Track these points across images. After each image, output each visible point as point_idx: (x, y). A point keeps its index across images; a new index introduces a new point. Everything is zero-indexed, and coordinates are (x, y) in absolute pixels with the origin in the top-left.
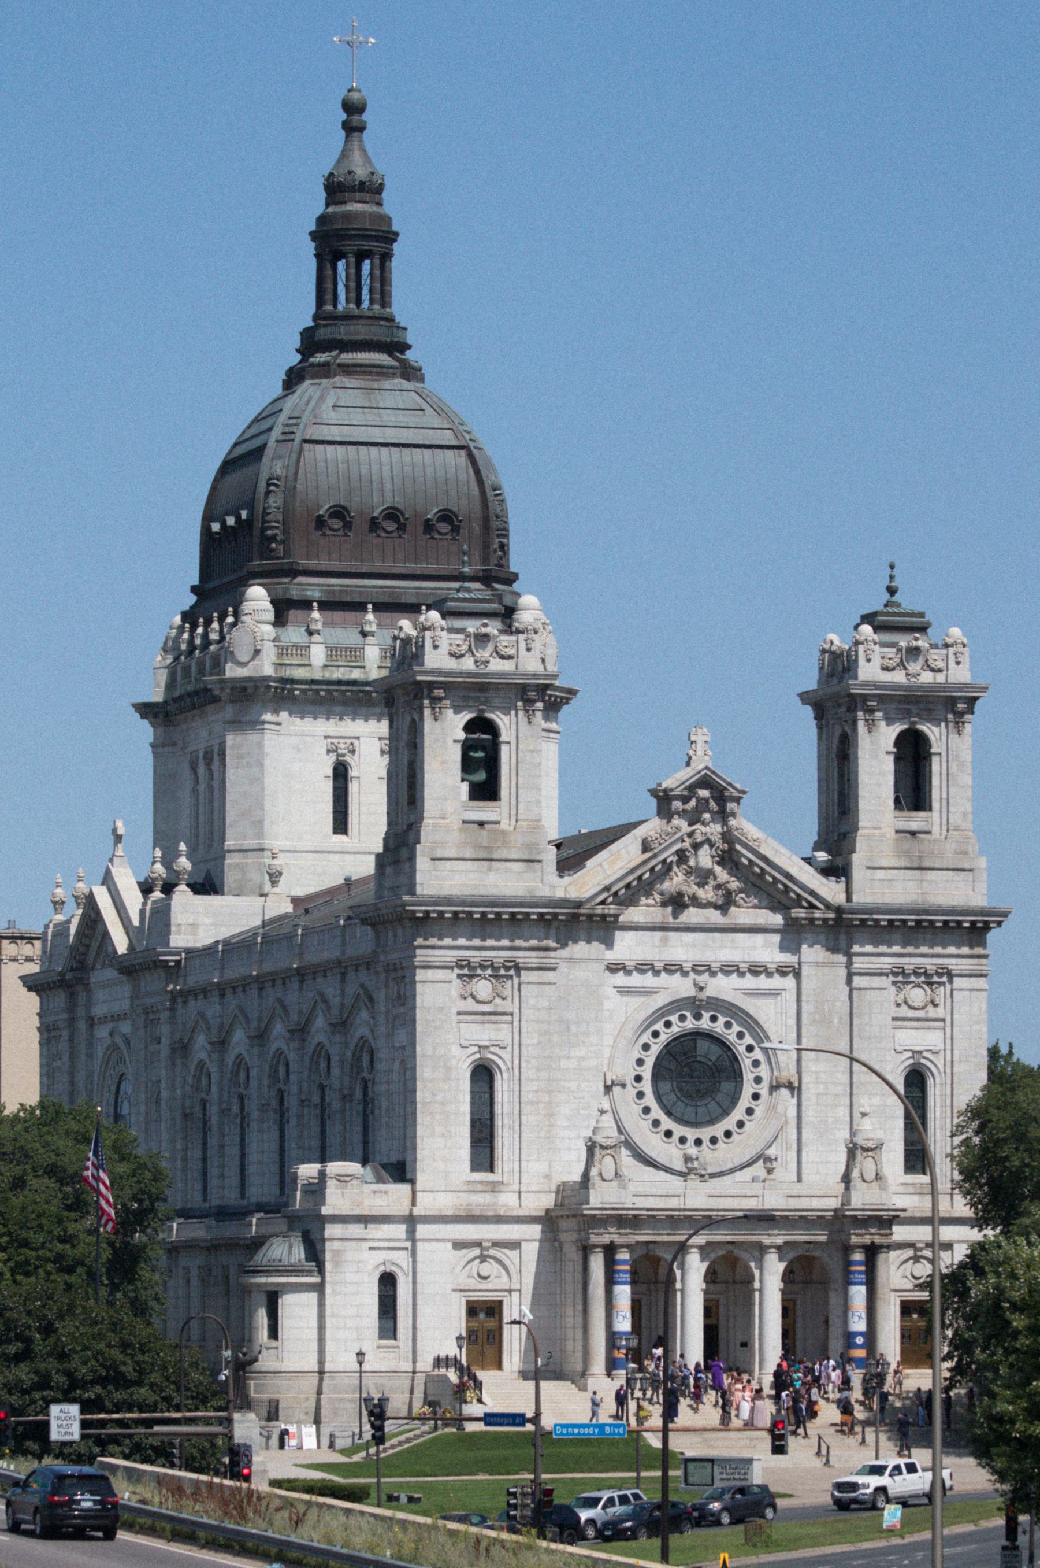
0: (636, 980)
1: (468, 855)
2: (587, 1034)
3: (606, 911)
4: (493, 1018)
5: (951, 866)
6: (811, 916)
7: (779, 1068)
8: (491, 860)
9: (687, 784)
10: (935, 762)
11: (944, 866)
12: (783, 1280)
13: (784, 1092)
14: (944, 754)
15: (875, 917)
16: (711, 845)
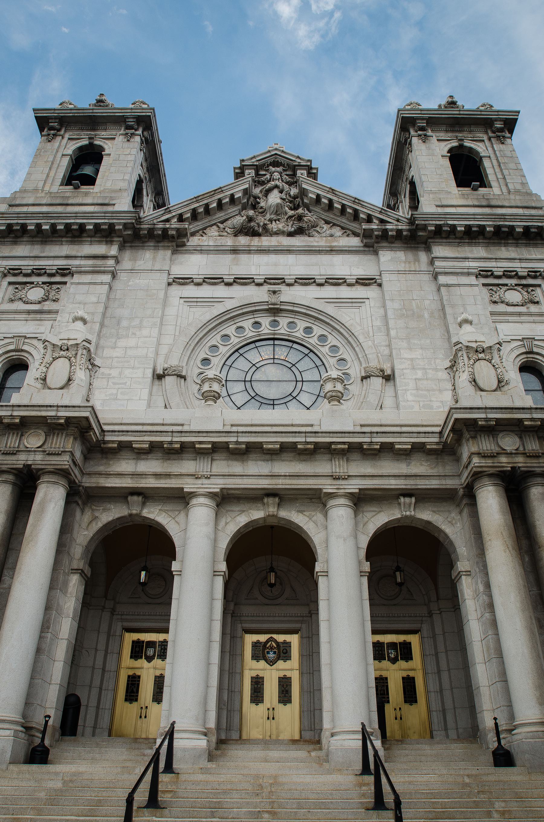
0: (206, 291)
1: (44, 202)
2: (140, 327)
3: (168, 226)
4: (38, 316)
5: (520, 205)
6: (383, 227)
7: (367, 360)
8: (67, 205)
9: (258, 159)
10: (486, 163)
11: (513, 204)
12: (369, 556)
13: (377, 382)
14: (492, 156)
15: (450, 222)
16: (281, 192)
